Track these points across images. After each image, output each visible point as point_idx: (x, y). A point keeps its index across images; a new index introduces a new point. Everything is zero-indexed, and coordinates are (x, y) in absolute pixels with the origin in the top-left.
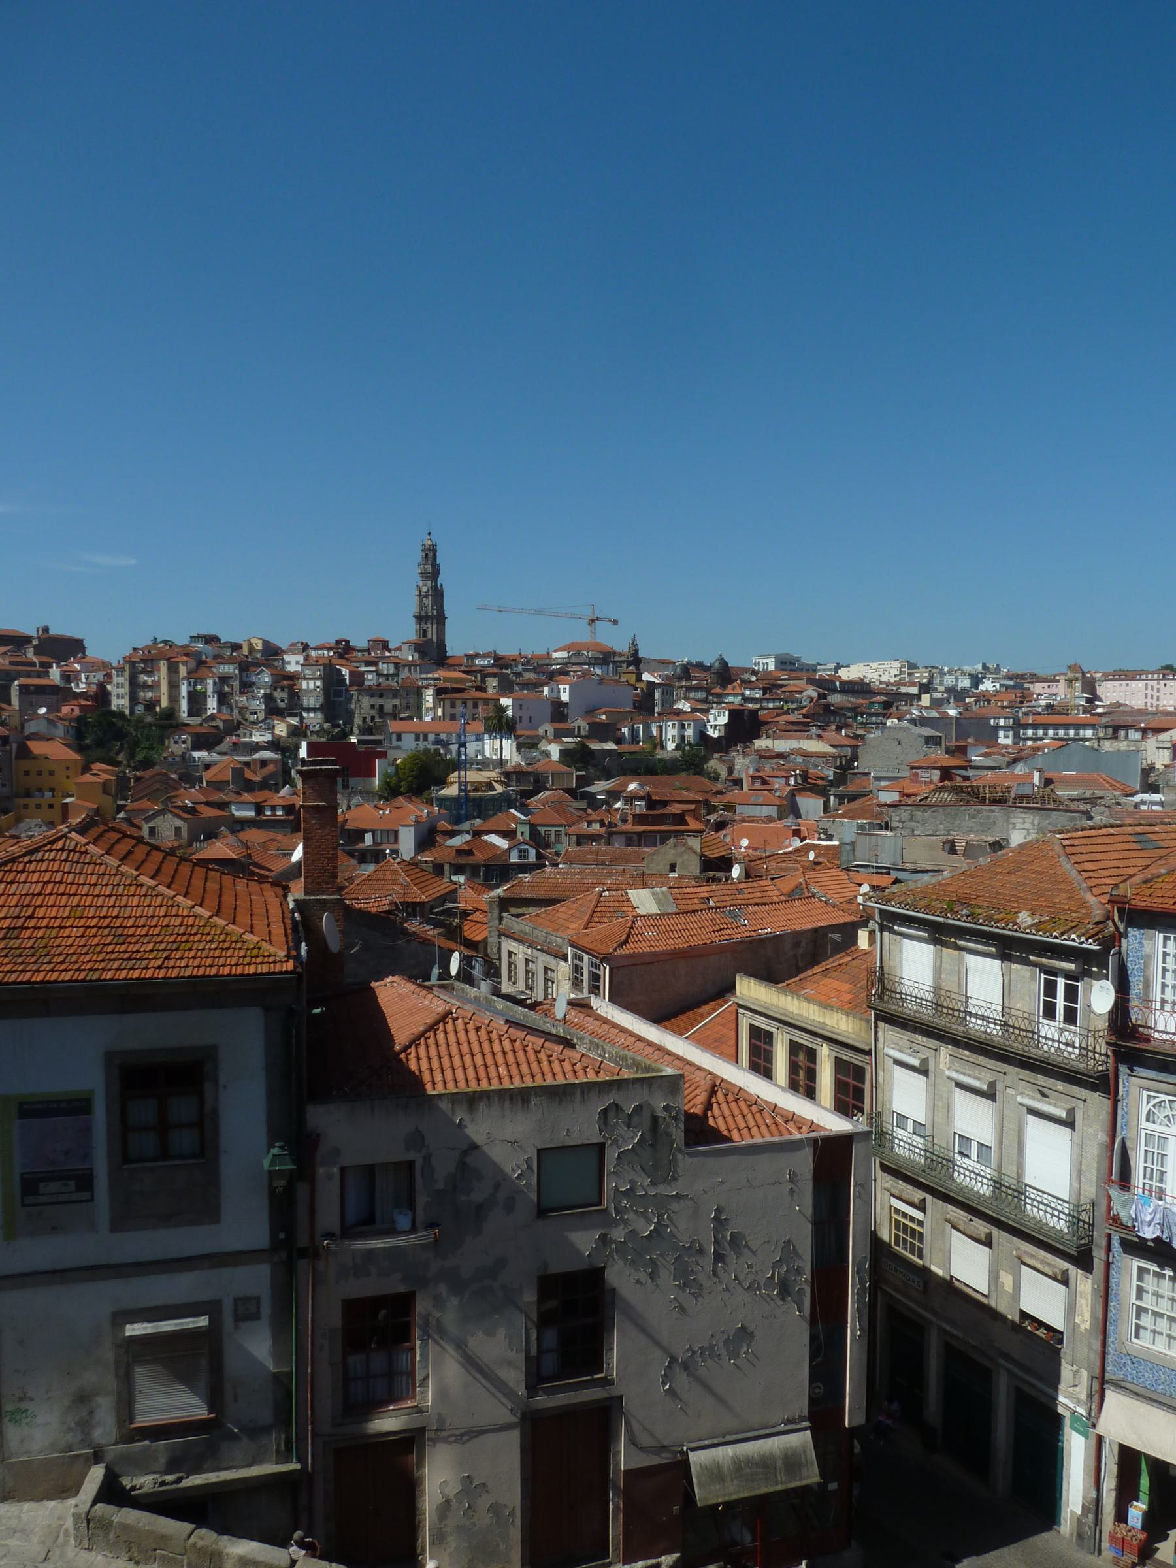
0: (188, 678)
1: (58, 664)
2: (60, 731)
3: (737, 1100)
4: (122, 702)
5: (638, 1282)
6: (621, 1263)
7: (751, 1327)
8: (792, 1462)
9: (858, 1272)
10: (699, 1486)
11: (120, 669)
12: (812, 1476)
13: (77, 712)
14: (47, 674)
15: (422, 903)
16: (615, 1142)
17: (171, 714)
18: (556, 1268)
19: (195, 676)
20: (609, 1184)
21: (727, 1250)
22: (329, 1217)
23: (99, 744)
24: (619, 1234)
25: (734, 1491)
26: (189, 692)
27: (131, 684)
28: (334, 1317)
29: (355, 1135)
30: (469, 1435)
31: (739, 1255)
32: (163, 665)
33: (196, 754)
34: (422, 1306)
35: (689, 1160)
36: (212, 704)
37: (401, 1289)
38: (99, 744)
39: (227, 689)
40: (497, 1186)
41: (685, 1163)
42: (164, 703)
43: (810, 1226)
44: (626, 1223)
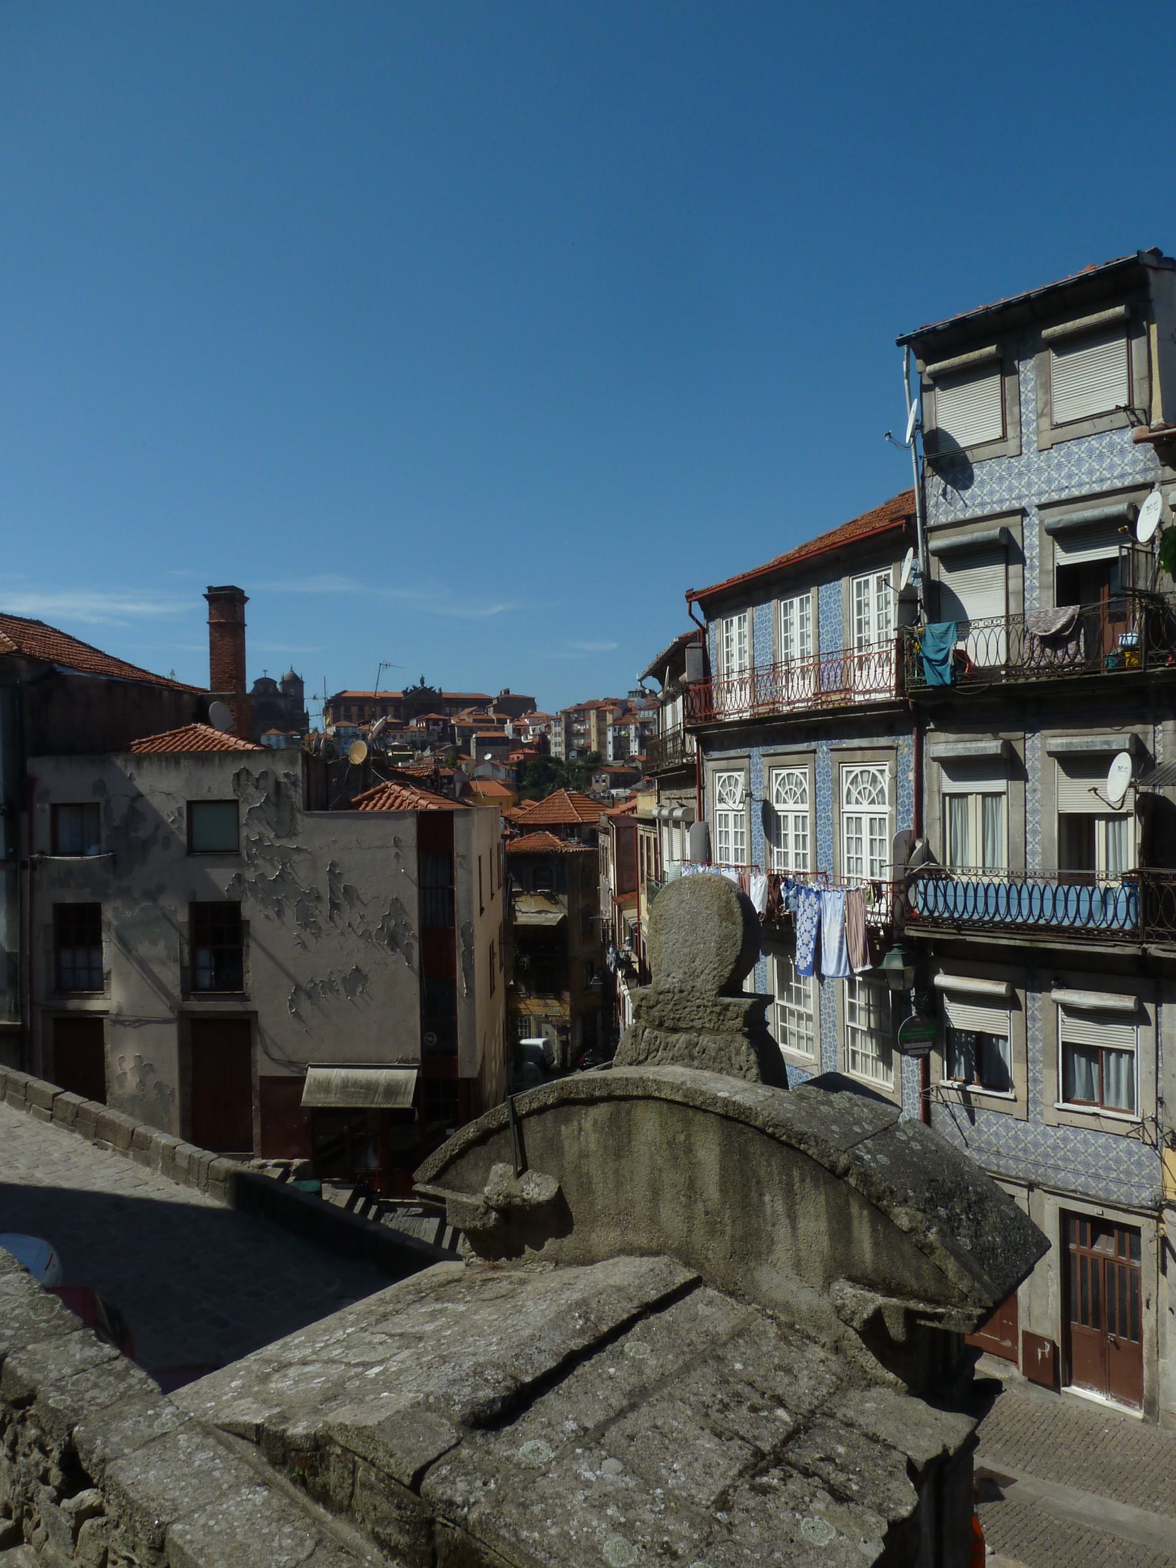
0: (613, 725)
1: (511, 721)
2: (502, 774)
3: (396, 798)
4: (559, 749)
5: (267, 917)
6: (252, 900)
7: (365, 970)
8: (392, 1090)
9: (463, 935)
10: (308, 1092)
11: (557, 720)
12: (406, 1102)
13: (522, 757)
14: (503, 729)
15: (579, 824)
16: (246, 800)
17: (598, 758)
18: (202, 898)
19: (619, 724)
20: (244, 832)
21: (341, 900)
22: (43, 838)
23: (535, 784)
24: (251, 876)
25: (334, 1101)
26: (614, 738)
27: (566, 733)
28: (45, 916)
29: (61, 781)
30: (140, 1022)
31: (352, 906)
32: (593, 714)
33: (614, 792)
34: (108, 914)
35: (307, 820)
36: (634, 748)
37: (90, 899)
38: (535, 784)
39: (647, 733)
40: (157, 827)
41: (304, 822)
42: (594, 748)
43: (415, 889)
44: (256, 866)
